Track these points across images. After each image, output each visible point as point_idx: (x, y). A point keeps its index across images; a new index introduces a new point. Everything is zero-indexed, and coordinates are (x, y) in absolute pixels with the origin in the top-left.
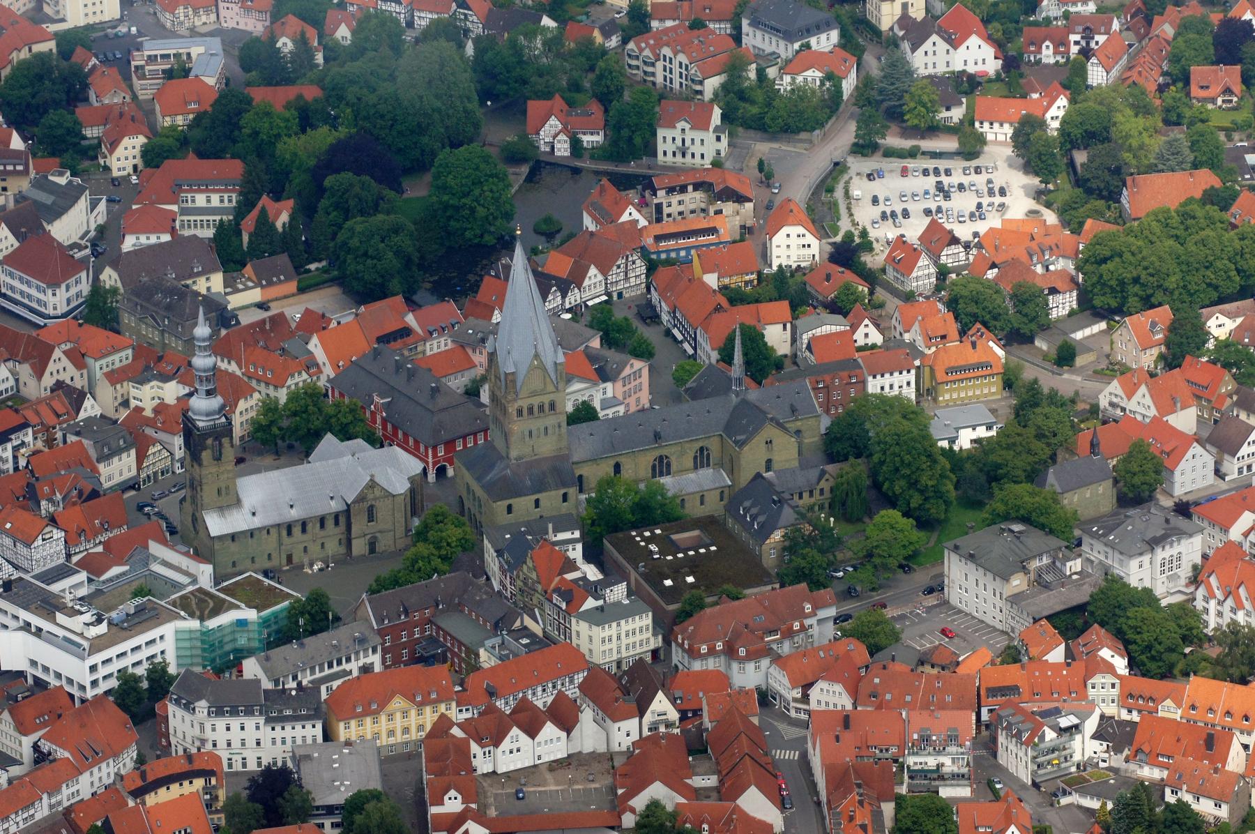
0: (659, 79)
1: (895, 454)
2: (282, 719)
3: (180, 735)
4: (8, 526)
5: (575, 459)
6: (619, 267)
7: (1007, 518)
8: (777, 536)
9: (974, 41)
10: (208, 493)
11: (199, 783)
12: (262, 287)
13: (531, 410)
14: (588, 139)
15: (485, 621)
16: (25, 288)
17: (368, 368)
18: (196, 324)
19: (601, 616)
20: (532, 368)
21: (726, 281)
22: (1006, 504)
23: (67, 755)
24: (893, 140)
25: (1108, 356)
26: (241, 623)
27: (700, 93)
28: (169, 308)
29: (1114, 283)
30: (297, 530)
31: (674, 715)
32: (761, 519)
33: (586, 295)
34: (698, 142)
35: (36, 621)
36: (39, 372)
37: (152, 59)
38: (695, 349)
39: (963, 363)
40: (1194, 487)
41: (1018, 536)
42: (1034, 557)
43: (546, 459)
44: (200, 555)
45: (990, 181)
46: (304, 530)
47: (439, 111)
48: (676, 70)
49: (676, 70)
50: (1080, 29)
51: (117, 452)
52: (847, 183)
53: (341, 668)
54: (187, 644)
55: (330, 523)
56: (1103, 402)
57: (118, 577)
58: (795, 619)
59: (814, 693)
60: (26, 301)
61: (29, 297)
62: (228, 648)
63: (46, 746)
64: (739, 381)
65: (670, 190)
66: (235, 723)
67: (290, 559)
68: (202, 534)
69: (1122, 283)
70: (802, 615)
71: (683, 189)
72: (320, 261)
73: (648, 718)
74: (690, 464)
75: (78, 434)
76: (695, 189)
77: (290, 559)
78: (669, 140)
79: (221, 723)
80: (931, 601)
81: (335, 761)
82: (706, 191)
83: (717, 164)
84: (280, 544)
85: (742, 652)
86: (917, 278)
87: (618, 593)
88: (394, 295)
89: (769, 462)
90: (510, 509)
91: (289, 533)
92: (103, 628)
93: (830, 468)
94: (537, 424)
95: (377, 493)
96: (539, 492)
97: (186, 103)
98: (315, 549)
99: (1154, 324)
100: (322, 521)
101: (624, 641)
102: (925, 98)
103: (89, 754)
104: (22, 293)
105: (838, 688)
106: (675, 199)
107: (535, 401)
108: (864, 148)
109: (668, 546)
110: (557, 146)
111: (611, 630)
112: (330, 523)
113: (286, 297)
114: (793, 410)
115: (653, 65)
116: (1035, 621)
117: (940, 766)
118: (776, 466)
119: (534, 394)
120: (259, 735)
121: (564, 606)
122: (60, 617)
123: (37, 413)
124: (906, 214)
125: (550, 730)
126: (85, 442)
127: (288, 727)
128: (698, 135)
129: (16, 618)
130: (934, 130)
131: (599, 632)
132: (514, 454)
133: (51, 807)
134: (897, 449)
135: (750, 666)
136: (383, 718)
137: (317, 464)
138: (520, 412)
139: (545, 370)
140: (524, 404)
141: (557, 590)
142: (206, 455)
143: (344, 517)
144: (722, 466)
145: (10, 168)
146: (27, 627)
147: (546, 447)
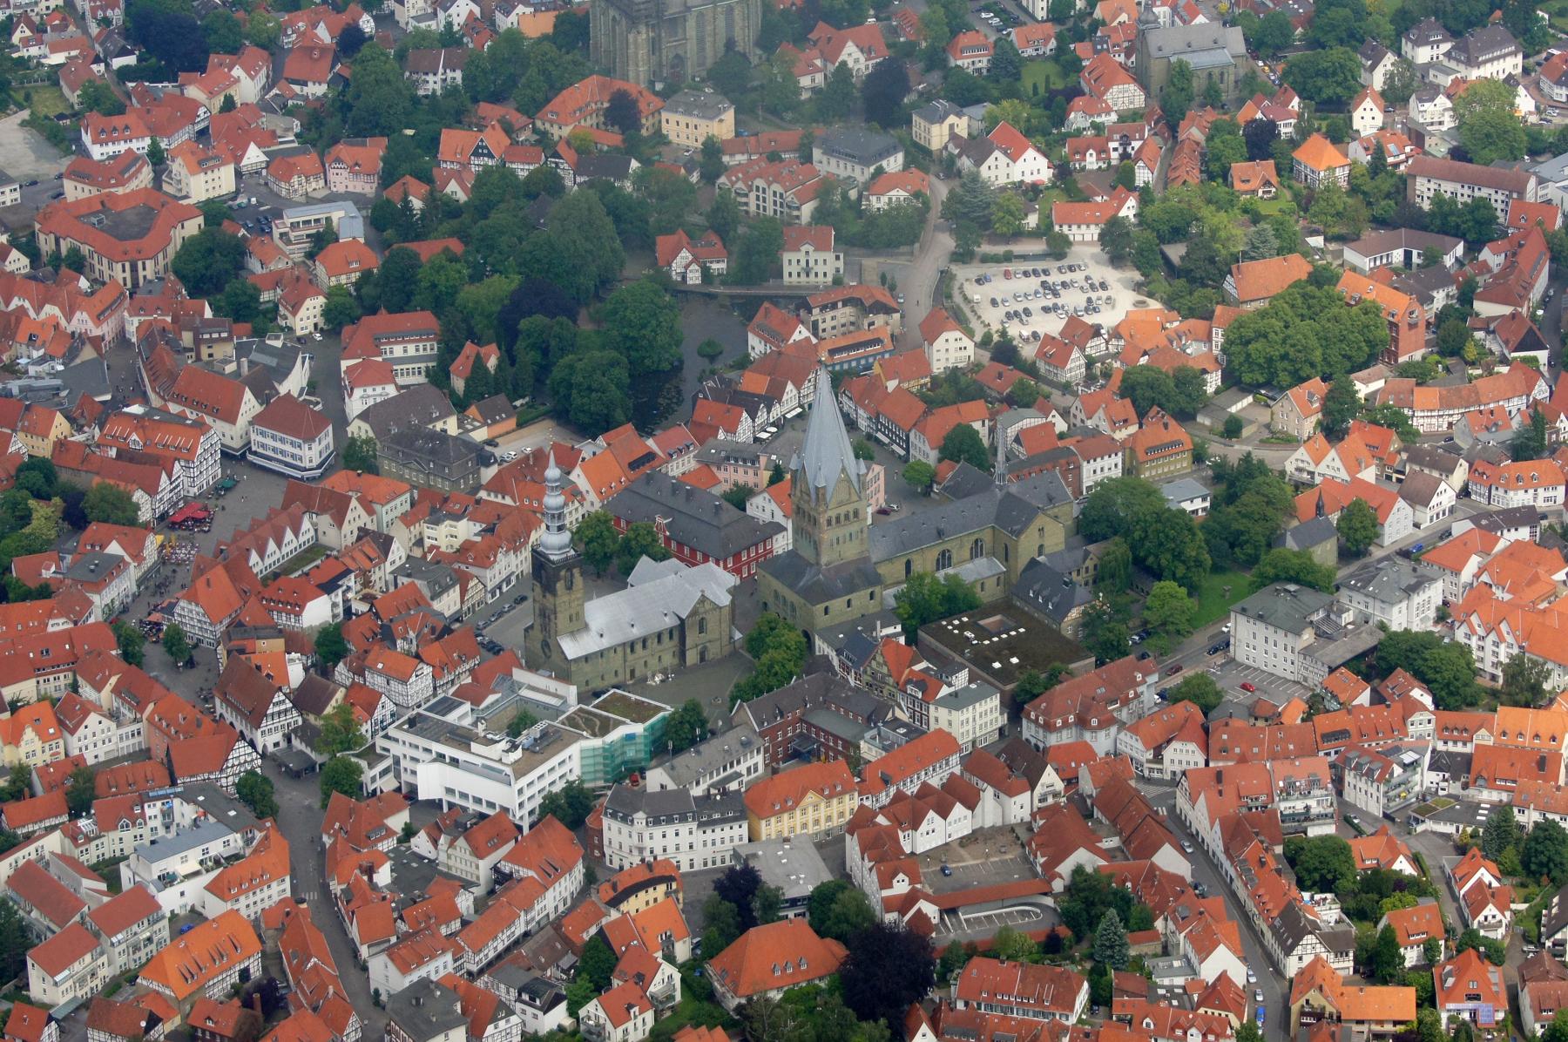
0: (752, 208)
1: (1158, 532)
2: (712, 823)
3: (615, 845)
4: (380, 666)
5: (874, 560)
7: (1277, 579)
8: (1074, 613)
9: (1031, 153)
10: (562, 620)
11: (662, 888)
13: (838, 519)
14: (718, 267)
15: (856, 716)
16: (278, 445)
17: (642, 492)
18: (546, 467)
19: (957, 701)
20: (840, 481)
22: (1275, 567)
23: (531, 873)
24: (986, 248)
25: (1268, 426)
26: (630, 738)
27: (798, 217)
28: (433, 452)
29: (1261, 361)
30: (639, 647)
31: (1060, 786)
32: (1055, 599)
33: (785, 409)
34: (820, 262)
35: (449, 751)
36: (339, 521)
37: (294, 226)
38: (907, 450)
40: (1398, 537)
41: (1293, 595)
44: (564, 676)
45: (1087, 278)
46: (644, 647)
47: (591, 252)
48: (770, 199)
49: (770, 199)
50: (1117, 136)
51: (446, 589)
52: (961, 288)
54: (591, 761)
55: (666, 638)
56: (1290, 467)
58: (1130, 688)
59: (1168, 753)
60: (280, 457)
61: (282, 452)
62: (618, 761)
63: (506, 867)
64: (1002, 477)
65: (823, 308)
66: (670, 830)
67: (632, 672)
68: (555, 657)
69: (1270, 360)
71: (834, 306)
72: (523, 397)
73: (1039, 790)
74: (967, 554)
75: (409, 576)
76: (844, 305)
77: (632, 672)
78: (794, 262)
79: (657, 831)
80: (1219, 659)
81: (781, 858)
82: (855, 305)
83: (837, 281)
85: (1094, 722)
86: (1071, 370)
87: (961, 679)
88: (620, 425)
89: (1041, 547)
90: (826, 611)
92: (518, 754)
93: (1091, 548)
94: (841, 532)
95: (707, 606)
96: (851, 592)
97: (349, 263)
98: (653, 662)
99: (1311, 395)
100: (659, 636)
101: (979, 722)
102: (1013, 208)
103: (551, 871)
104: (274, 450)
105: (1192, 746)
106: (829, 315)
107: (842, 511)
108: (963, 256)
109: (982, 633)
110: (689, 275)
111: (968, 713)
112: (666, 638)
113: (508, 433)
114: (1050, 499)
115: (746, 195)
116: (1332, 670)
118: (1047, 550)
119: (840, 504)
120: (692, 839)
121: (920, 695)
122: (475, 747)
123: (353, 559)
124: (1027, 312)
126: (419, 583)
127: (718, 830)
128: (821, 256)
129: (428, 750)
130: (1019, 234)
131: (957, 716)
132: (824, 560)
133: (527, 923)
134: (1159, 526)
135: (1102, 734)
136: (798, 812)
137: (647, 586)
138: (829, 522)
139: (850, 481)
140: (832, 514)
141: (908, 681)
142: (560, 586)
143: (680, 631)
144: (994, 554)
145: (215, 336)
146: (441, 757)
147: (851, 551)
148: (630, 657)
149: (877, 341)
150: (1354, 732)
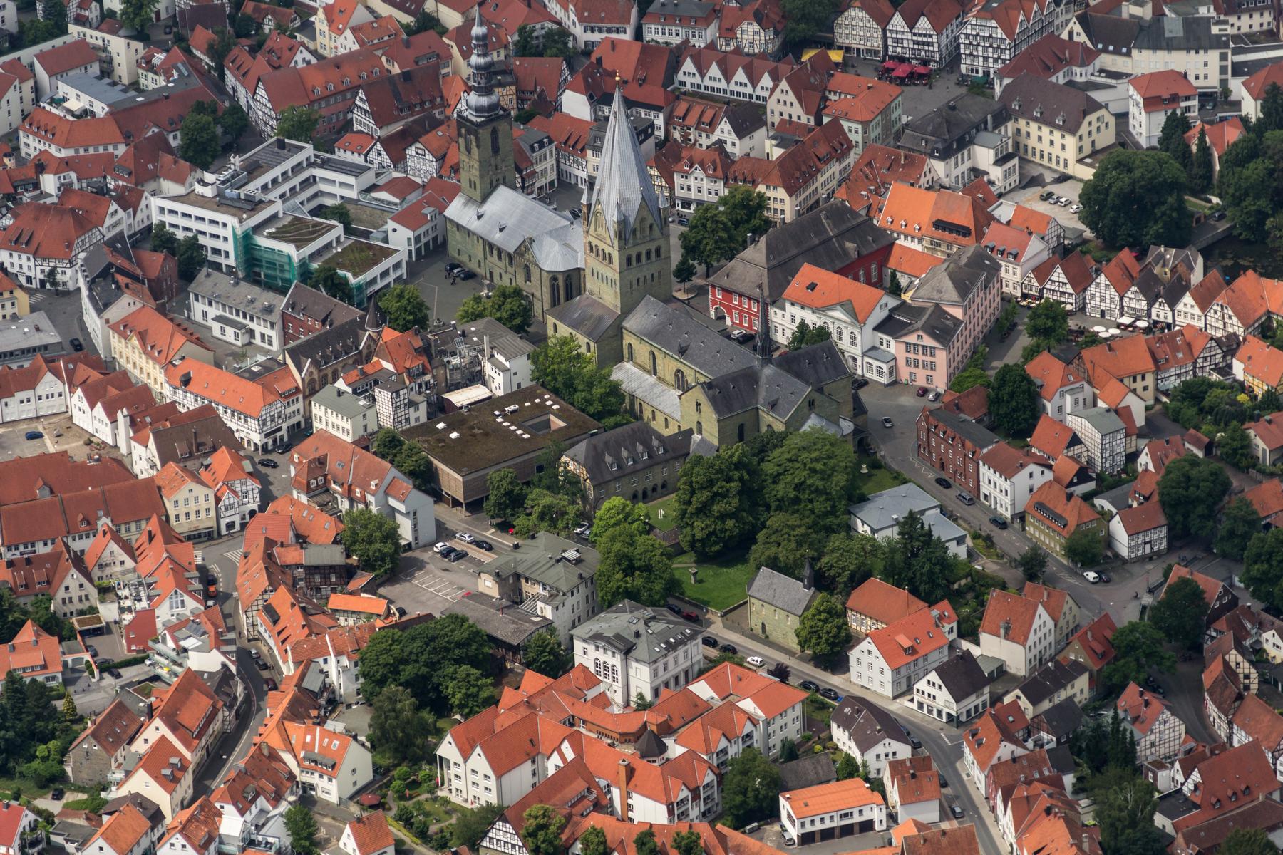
39: (1051, 506)
42: (538, 582)
43: (604, 306)
57: (382, 201)
70: (365, 488)
84: (485, 258)
91: (492, 253)
107: (601, 246)
119: (598, 237)
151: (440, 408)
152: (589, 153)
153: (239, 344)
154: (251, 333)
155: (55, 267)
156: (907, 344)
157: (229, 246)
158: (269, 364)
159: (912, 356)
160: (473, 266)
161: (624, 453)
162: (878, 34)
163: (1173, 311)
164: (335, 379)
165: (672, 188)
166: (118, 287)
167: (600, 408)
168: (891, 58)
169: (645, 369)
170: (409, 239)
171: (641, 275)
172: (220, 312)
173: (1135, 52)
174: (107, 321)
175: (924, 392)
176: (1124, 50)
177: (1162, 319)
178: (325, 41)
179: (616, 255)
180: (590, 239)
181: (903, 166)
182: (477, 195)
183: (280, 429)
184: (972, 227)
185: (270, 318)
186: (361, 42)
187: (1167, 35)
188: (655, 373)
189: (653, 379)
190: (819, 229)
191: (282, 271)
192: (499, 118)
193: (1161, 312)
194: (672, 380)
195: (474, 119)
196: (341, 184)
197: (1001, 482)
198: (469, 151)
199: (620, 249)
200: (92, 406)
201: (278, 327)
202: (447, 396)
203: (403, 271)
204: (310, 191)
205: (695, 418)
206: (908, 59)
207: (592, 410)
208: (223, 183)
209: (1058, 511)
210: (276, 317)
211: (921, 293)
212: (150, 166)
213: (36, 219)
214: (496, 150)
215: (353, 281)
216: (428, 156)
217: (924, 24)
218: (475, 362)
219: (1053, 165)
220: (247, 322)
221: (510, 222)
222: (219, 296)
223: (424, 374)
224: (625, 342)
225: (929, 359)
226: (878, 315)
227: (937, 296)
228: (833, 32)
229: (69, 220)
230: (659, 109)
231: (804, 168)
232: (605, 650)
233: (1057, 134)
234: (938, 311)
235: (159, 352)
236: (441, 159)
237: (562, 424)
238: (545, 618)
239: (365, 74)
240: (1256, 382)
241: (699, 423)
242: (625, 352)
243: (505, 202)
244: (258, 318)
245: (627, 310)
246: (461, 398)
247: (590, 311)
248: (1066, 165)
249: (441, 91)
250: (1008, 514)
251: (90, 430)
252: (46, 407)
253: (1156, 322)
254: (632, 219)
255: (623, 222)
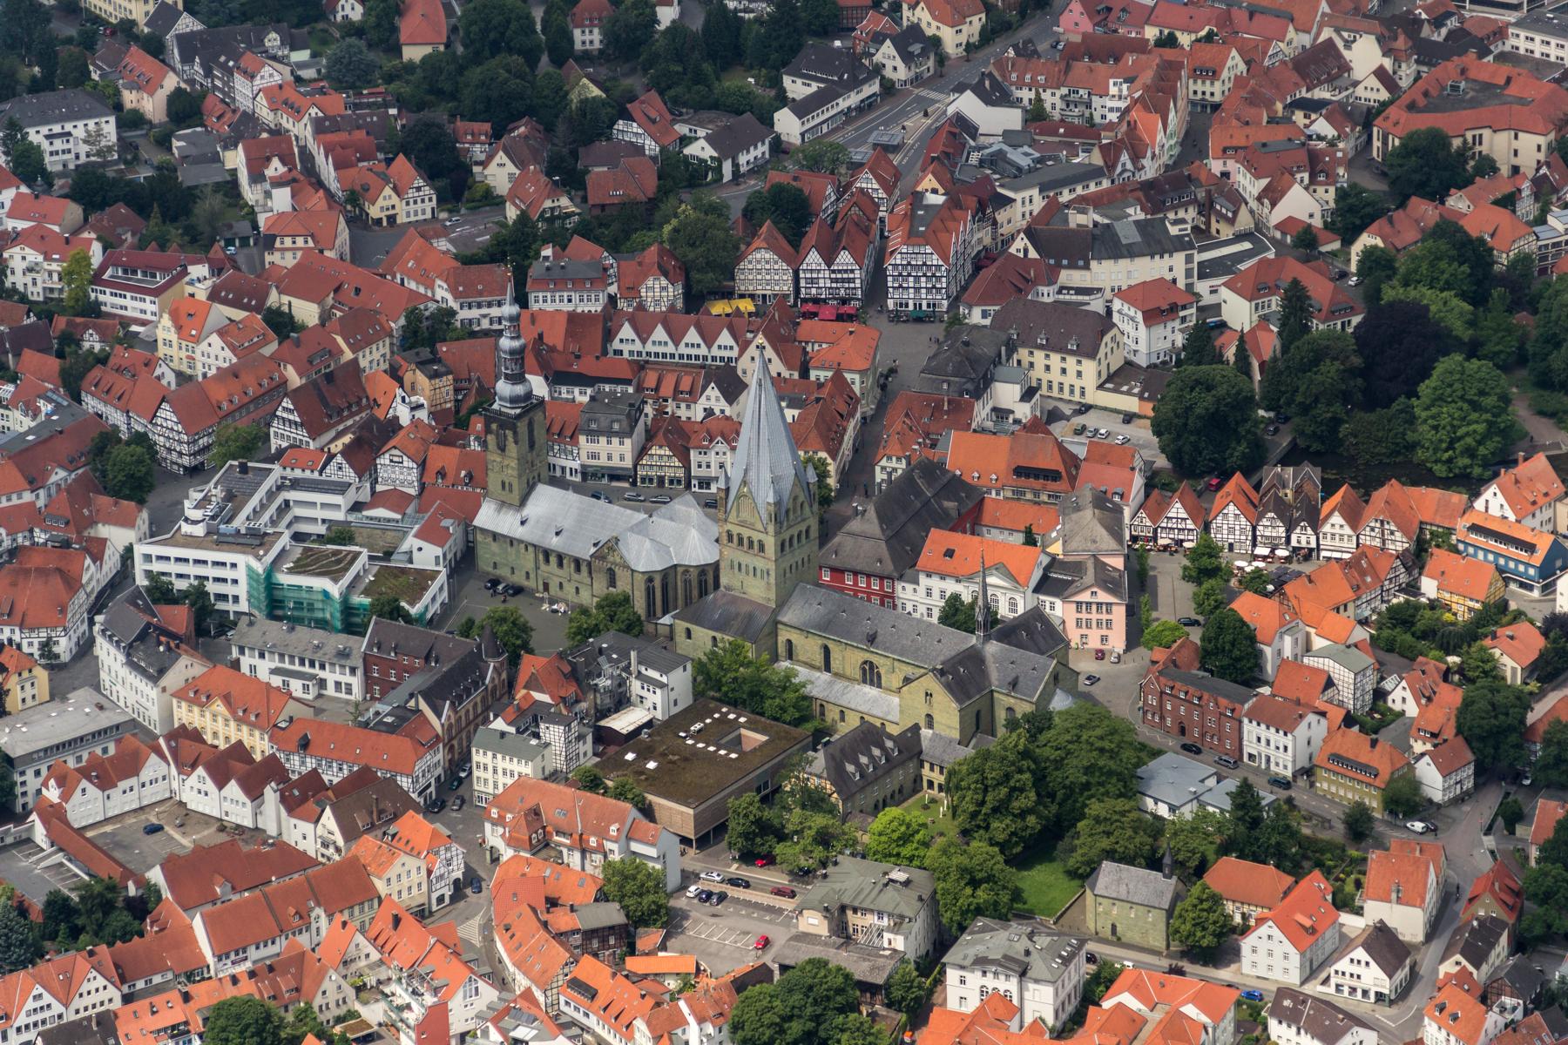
6: (1373, 529)
12: (1141, 397)
21: (1447, 596)
26: (326, 593)
39: (1351, 756)
42: (872, 911)
43: (751, 602)
53: (311, 671)
57: (379, 519)
66: (113, 650)
70: (603, 835)
84: (537, 568)
91: (547, 561)
98: (569, 589)
107: (746, 533)
117: (408, 1007)
119: (742, 524)
125: (233, 788)
148: (543, 566)
149: (1530, 548)
150: (601, 1000)
151: (604, 737)
152: (582, 439)
153: (310, 697)
154: (322, 683)
155: (49, 638)
156: (1079, 604)
157: (242, 590)
158: (399, 712)
159: (1084, 616)
160: (518, 579)
161: (864, 760)
162: (789, 276)
163: (1317, 535)
164: (486, 721)
165: (687, 468)
166: (169, 649)
167: (797, 715)
168: (805, 301)
169: (812, 667)
170: (437, 558)
171: (792, 561)
172: (276, 664)
173: (1093, 264)
174: (164, 690)
175: (1100, 655)
176: (1081, 263)
177: (1304, 544)
178: (174, 351)
179: (770, 542)
180: (729, 527)
181: (948, 412)
182: (515, 497)
183: (429, 786)
184: (1061, 469)
185: (348, 663)
186: (233, 349)
187: (1124, 242)
188: (828, 668)
189: (826, 676)
190: (918, 493)
191: (311, 608)
192: (534, 407)
193: (1303, 537)
194: (858, 674)
195: (512, 412)
196: (323, 505)
197: (1278, 738)
198: (502, 448)
199: (777, 533)
200: (221, 785)
201: (360, 672)
202: (603, 723)
203: (445, 594)
204: (288, 518)
205: (925, 710)
206: (824, 300)
207: (788, 718)
208: (213, 518)
209: (1363, 759)
210: (359, 664)
211: (1074, 545)
212: (86, 512)
213: (14, 584)
214: (532, 445)
215: (414, 611)
216: (407, 463)
217: (844, 259)
218: (622, 683)
219: (1066, 395)
220: (316, 671)
221: (567, 523)
222: (274, 646)
223: (577, 701)
224: (782, 639)
225: (1104, 617)
226: (1037, 575)
227: (1093, 547)
228: (733, 279)
229: (57, 581)
230: (628, 382)
231: (835, 428)
232: (996, 974)
233: (1071, 361)
234: (1100, 566)
235: (257, 716)
236: (422, 466)
237: (764, 738)
238: (895, 951)
239: (265, 382)
240: (1455, 598)
241: (928, 716)
242: (782, 649)
243: (545, 501)
244: (333, 664)
245: (782, 603)
246: (623, 722)
247: (733, 609)
248: (1083, 394)
249: (364, 390)
250: (1289, 773)
251: (216, 813)
252: (151, 795)
253: (1295, 549)
254: (785, 498)
255: (778, 504)
